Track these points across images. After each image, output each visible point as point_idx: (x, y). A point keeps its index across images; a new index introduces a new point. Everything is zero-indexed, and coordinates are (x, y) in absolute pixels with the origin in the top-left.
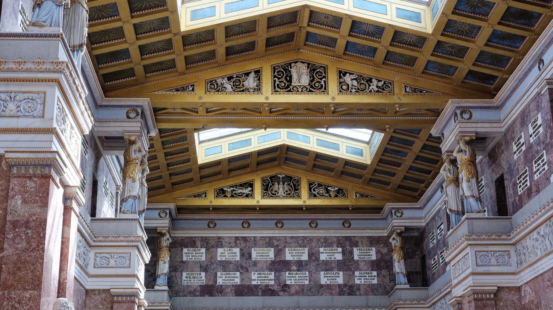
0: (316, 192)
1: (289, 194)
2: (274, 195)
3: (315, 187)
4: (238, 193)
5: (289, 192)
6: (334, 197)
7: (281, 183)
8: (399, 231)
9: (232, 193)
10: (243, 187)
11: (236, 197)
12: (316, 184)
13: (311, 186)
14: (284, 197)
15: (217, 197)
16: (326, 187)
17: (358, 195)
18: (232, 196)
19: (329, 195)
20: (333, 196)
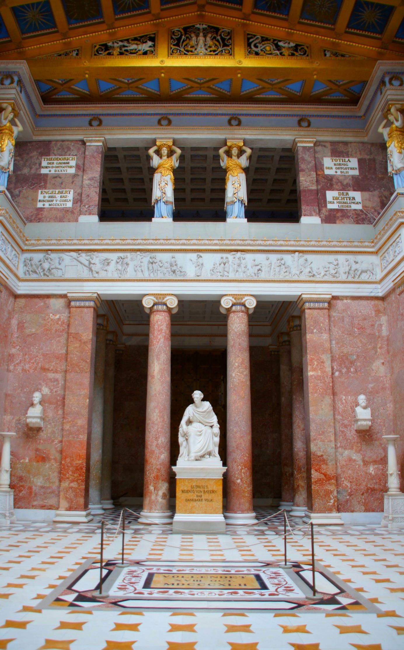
0: (259, 49)
1: (214, 51)
2: (188, 52)
3: (257, 41)
4: (131, 50)
5: (213, 48)
6: (289, 55)
7: (201, 34)
8: (398, 106)
9: (121, 49)
10: (139, 41)
11: (126, 55)
12: (258, 38)
13: (251, 40)
14: (206, 54)
15: (95, 55)
16: (276, 42)
17: (328, 54)
18: (121, 54)
19: (281, 54)
20: (286, 54)
